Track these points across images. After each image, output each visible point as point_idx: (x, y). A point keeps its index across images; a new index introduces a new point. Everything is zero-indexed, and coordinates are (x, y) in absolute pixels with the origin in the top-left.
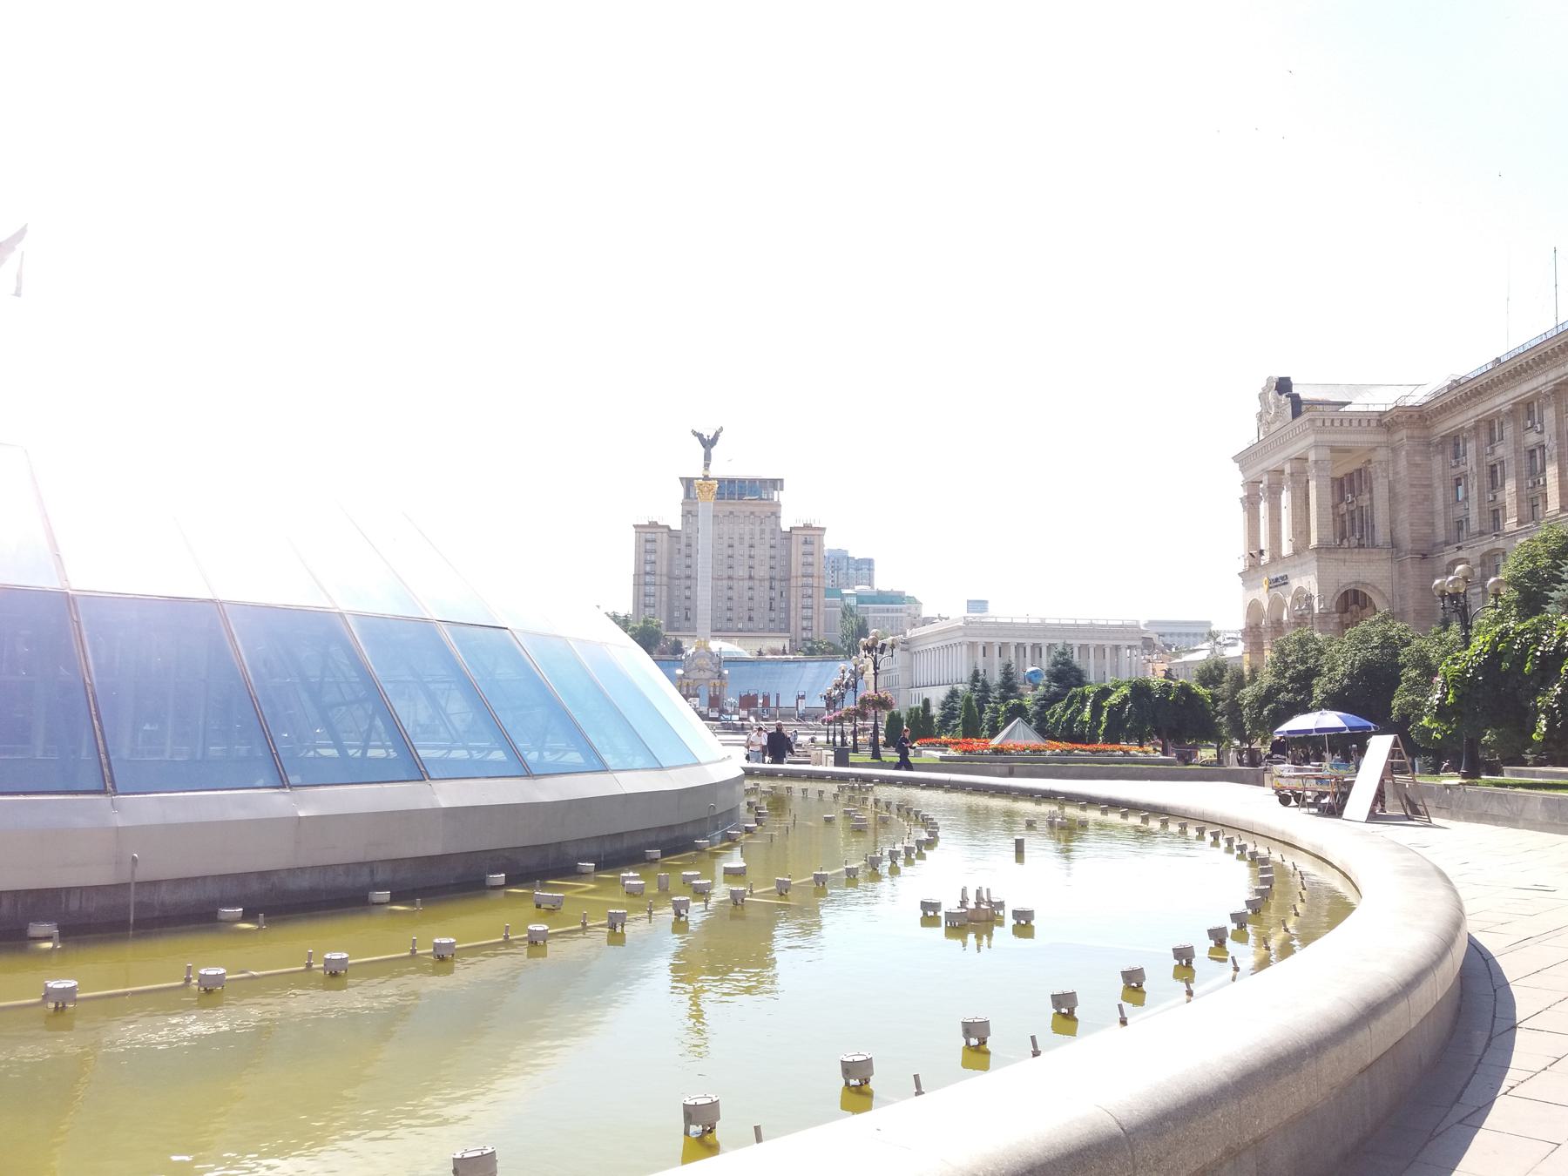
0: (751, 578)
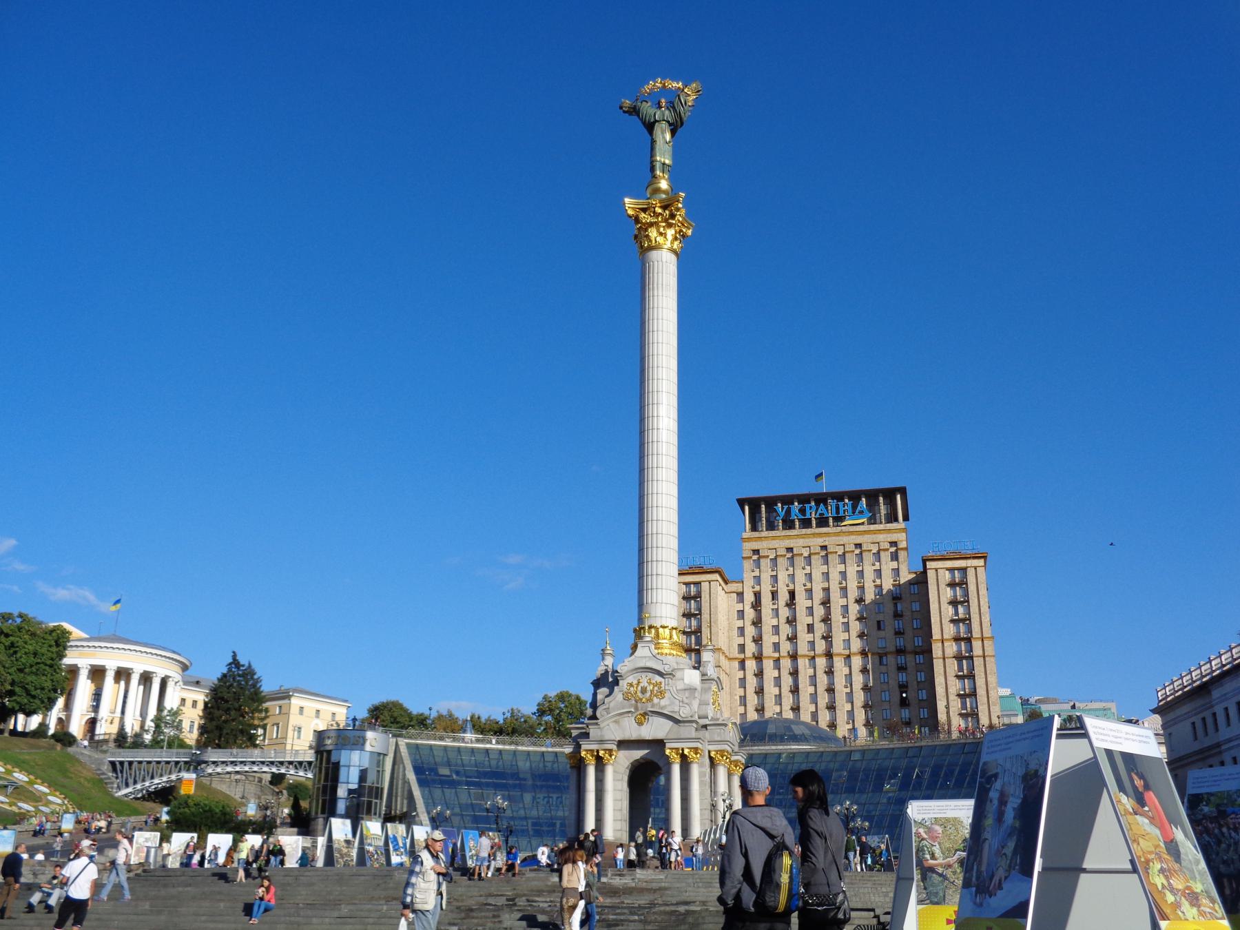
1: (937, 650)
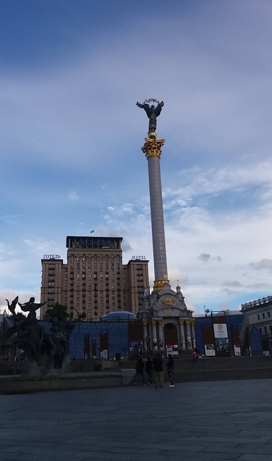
1: (133, 290)
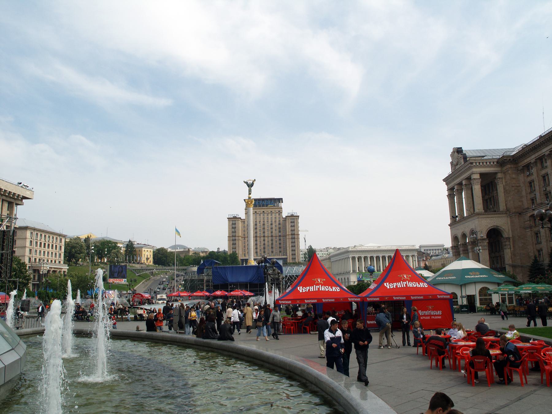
0: (272, 236)
1: (288, 237)
